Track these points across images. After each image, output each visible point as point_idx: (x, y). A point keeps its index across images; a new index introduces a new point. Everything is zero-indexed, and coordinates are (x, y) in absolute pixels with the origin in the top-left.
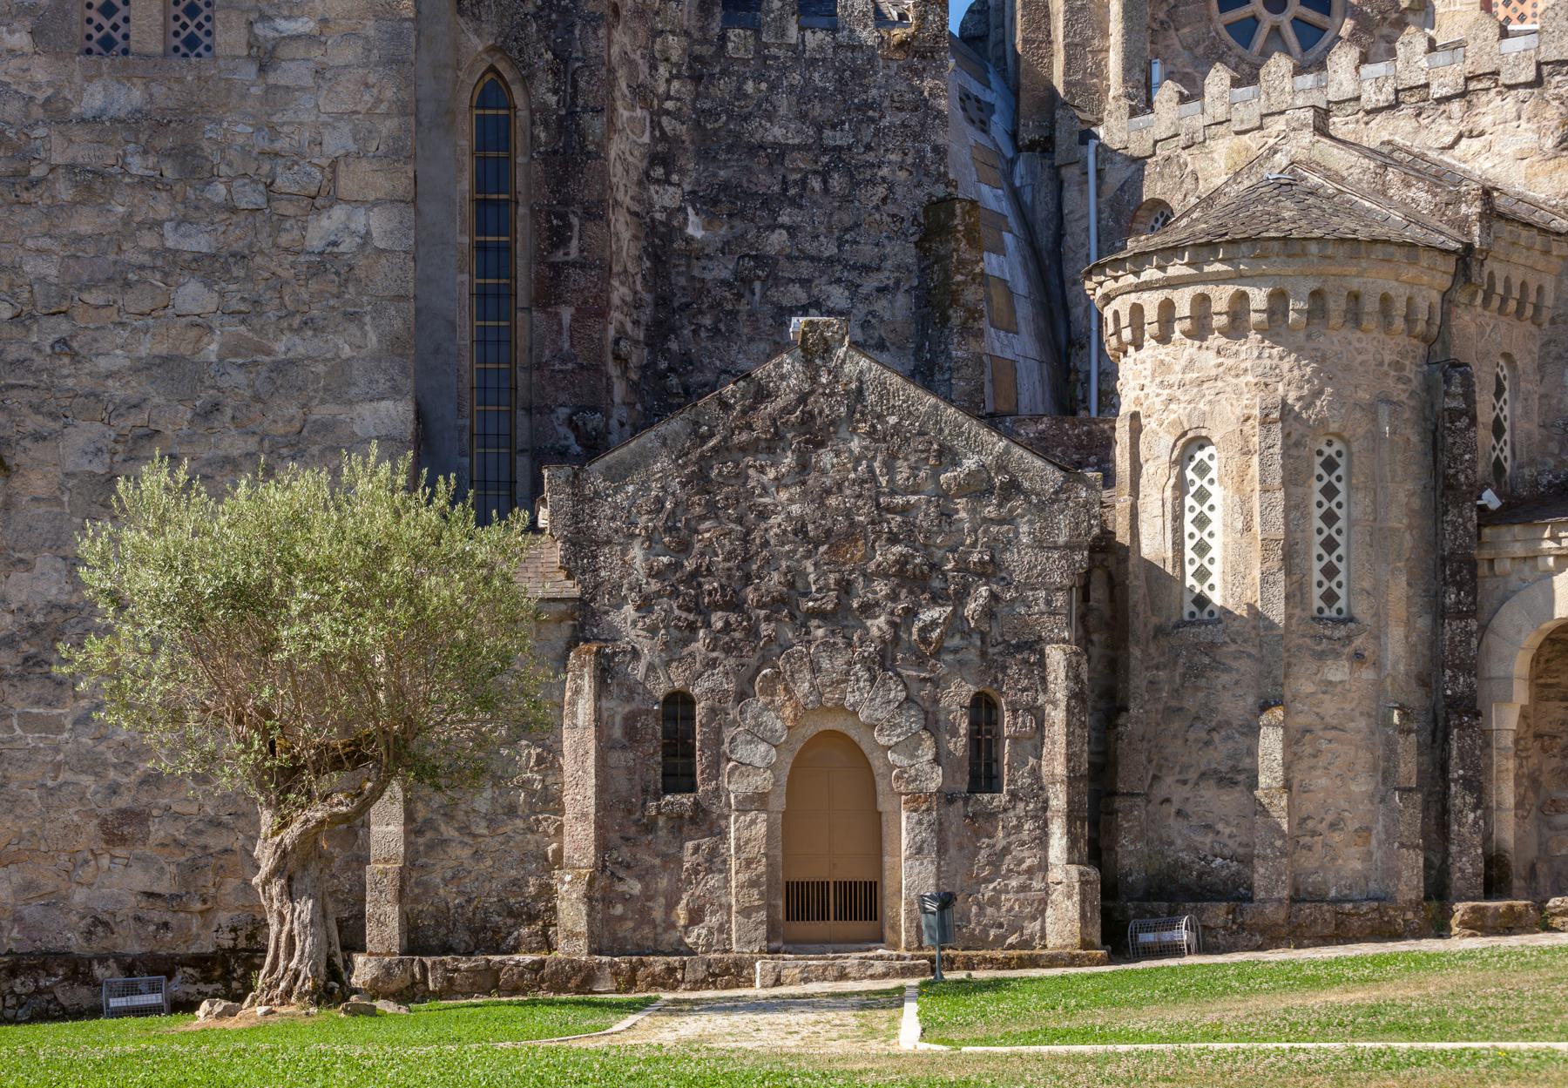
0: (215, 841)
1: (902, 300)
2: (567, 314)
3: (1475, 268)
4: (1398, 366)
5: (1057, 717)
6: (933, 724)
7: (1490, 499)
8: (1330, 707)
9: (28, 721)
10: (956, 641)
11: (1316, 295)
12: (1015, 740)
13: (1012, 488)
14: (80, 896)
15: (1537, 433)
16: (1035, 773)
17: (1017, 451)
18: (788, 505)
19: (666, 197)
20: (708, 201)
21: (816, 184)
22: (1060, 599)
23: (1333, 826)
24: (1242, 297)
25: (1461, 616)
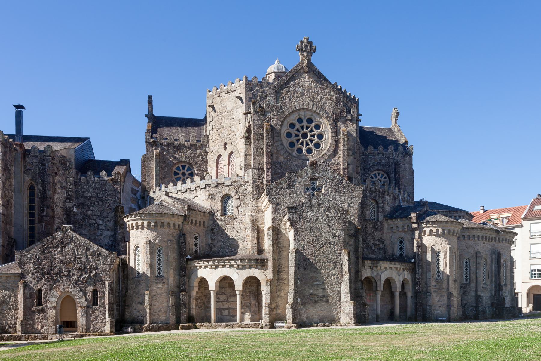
2: (44, 224)
3: (187, 219)
4: (172, 235)
5: (107, 293)
6: (85, 294)
7: (189, 257)
8: (159, 291)
10: (90, 280)
11: (156, 223)
12: (100, 297)
13: (99, 254)
15: (205, 246)
16: (104, 302)
17: (101, 248)
18: (59, 257)
19: (70, 205)
20: (77, 206)
21: (97, 203)
22: (108, 273)
23: (159, 311)
24: (143, 223)
25: (183, 276)
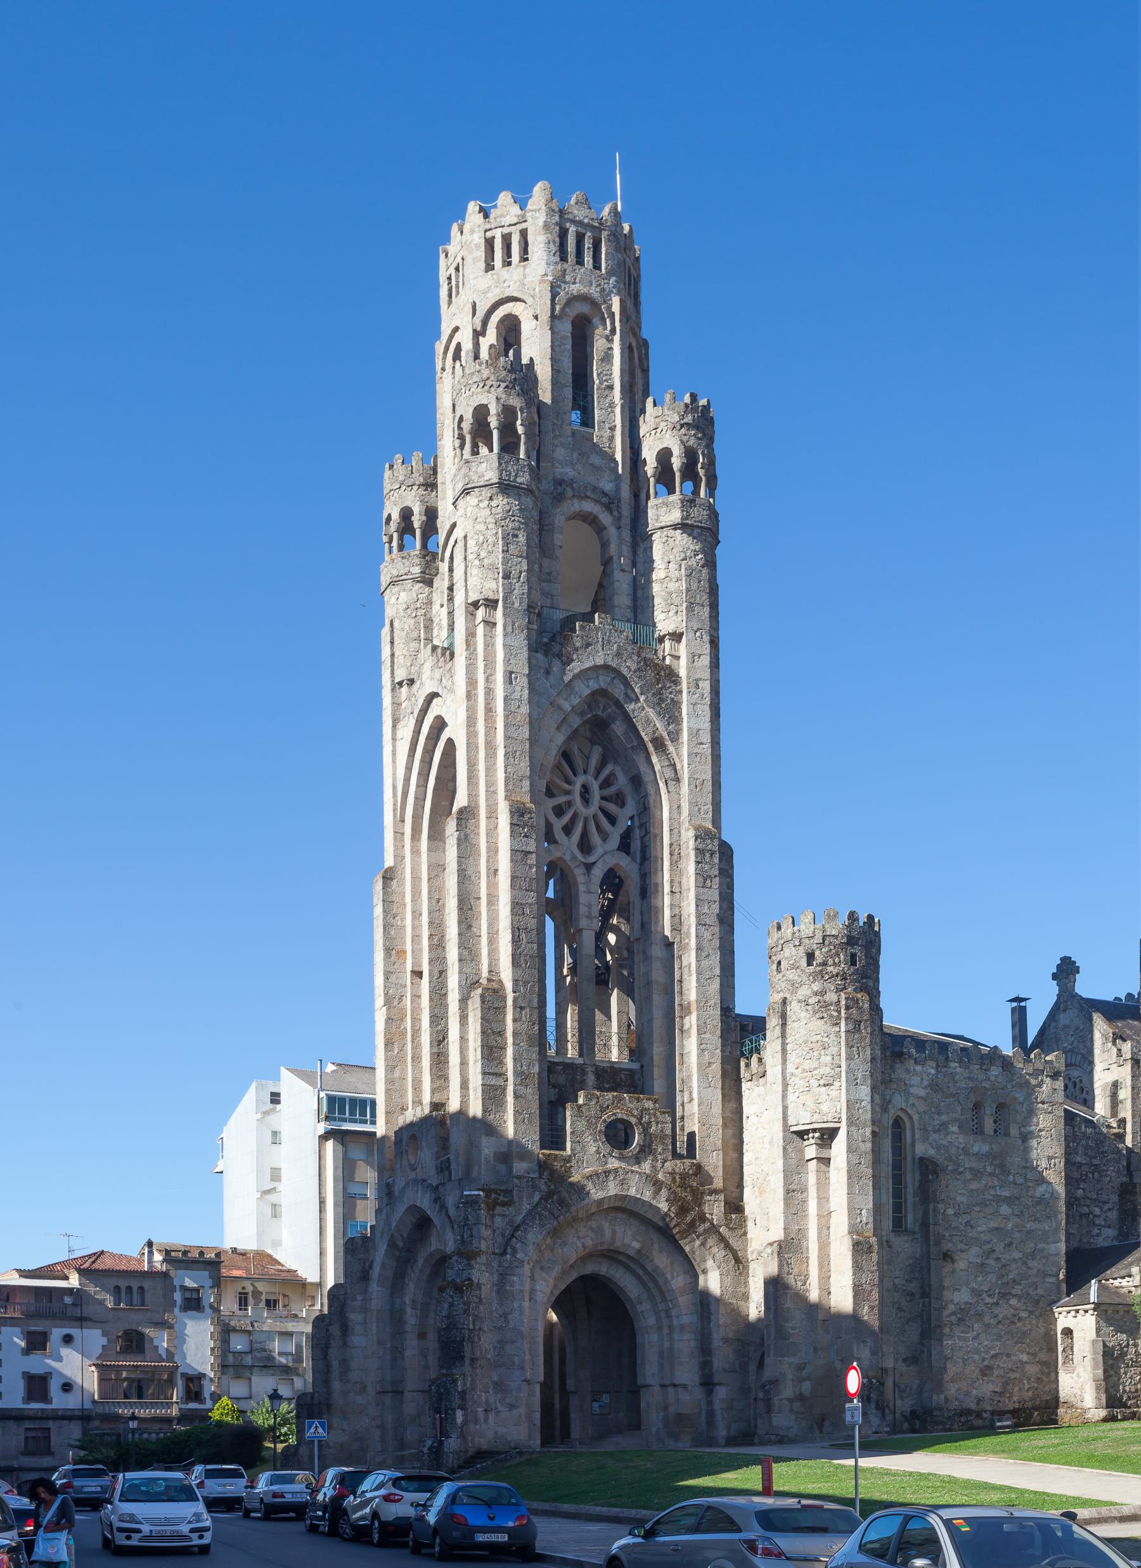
0: (1012, 1376)
1: (1115, 1213)
9: (960, 1338)
14: (975, 1392)
